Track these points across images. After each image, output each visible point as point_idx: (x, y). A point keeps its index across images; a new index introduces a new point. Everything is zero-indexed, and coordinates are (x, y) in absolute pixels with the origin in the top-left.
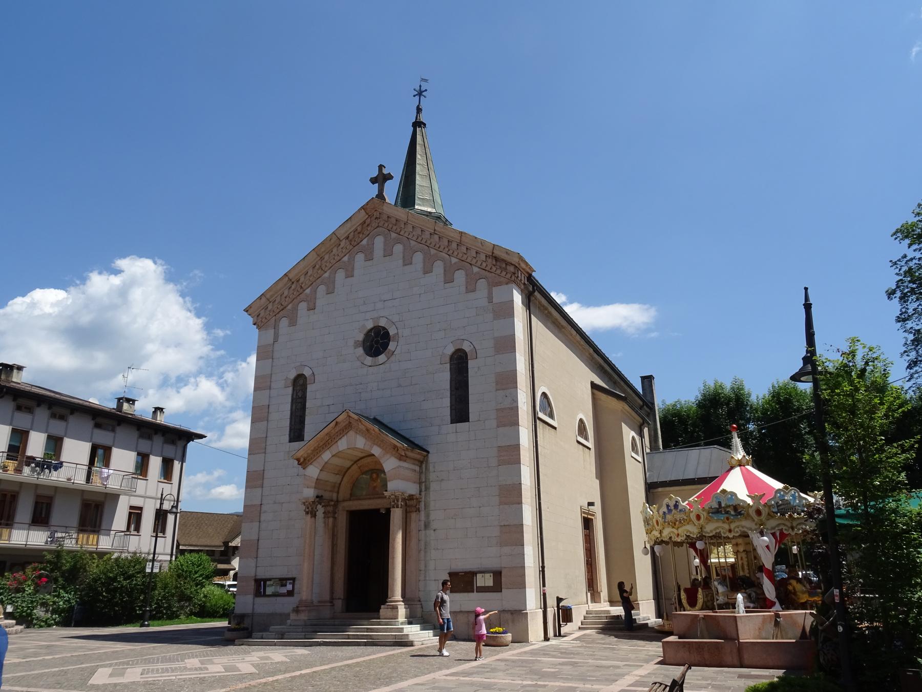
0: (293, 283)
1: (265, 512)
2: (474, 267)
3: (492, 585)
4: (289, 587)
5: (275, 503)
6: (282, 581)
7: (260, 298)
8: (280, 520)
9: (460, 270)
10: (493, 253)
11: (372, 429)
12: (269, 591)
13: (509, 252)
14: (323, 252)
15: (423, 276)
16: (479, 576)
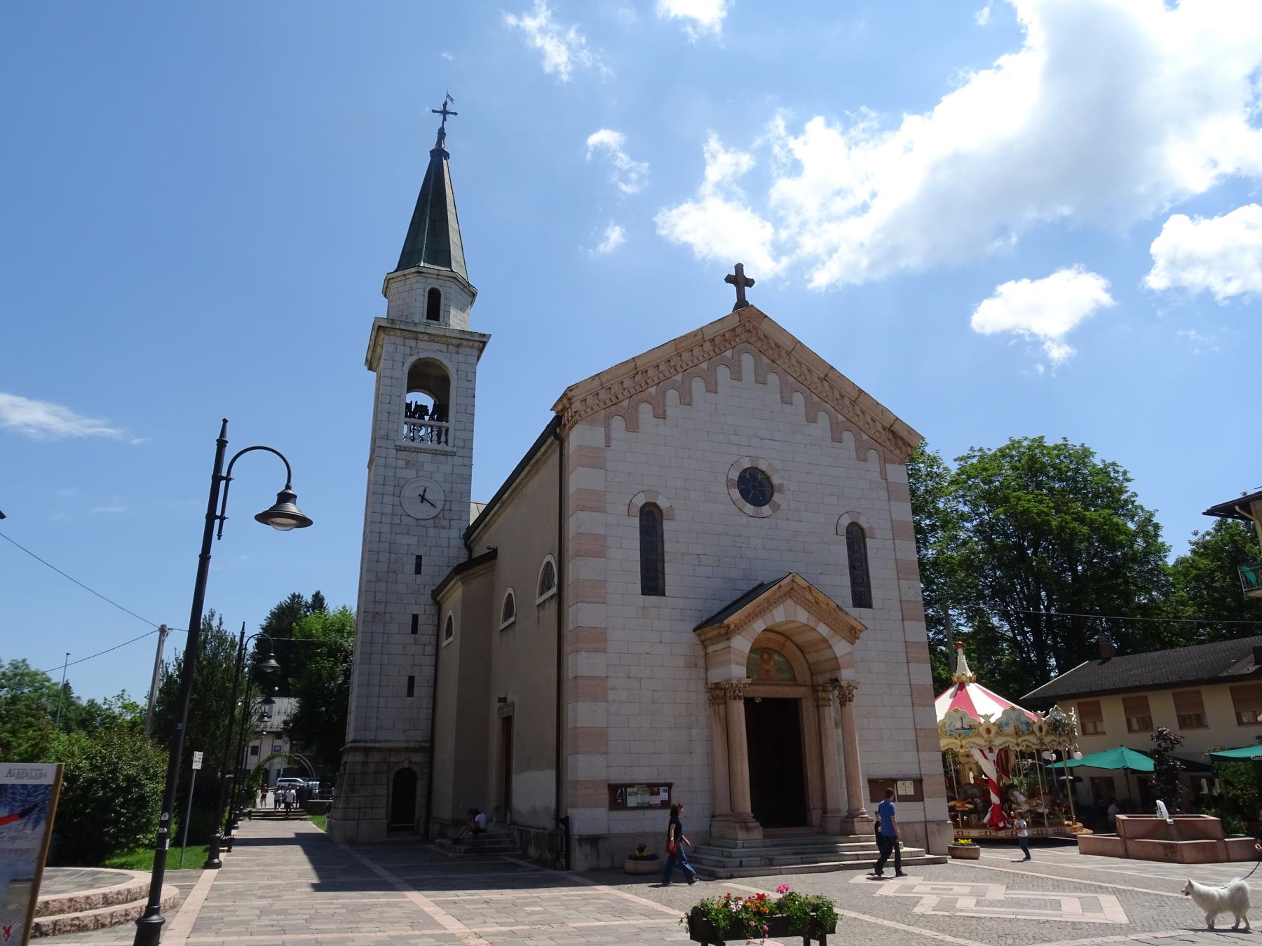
0: (637, 373)
1: (614, 688)
2: (863, 434)
3: (913, 794)
4: (664, 796)
5: (629, 677)
6: (653, 788)
7: (593, 378)
8: (640, 703)
9: (848, 432)
10: (891, 426)
11: (826, 603)
12: (632, 801)
13: (912, 432)
14: (682, 348)
15: (806, 423)
16: (899, 783)
